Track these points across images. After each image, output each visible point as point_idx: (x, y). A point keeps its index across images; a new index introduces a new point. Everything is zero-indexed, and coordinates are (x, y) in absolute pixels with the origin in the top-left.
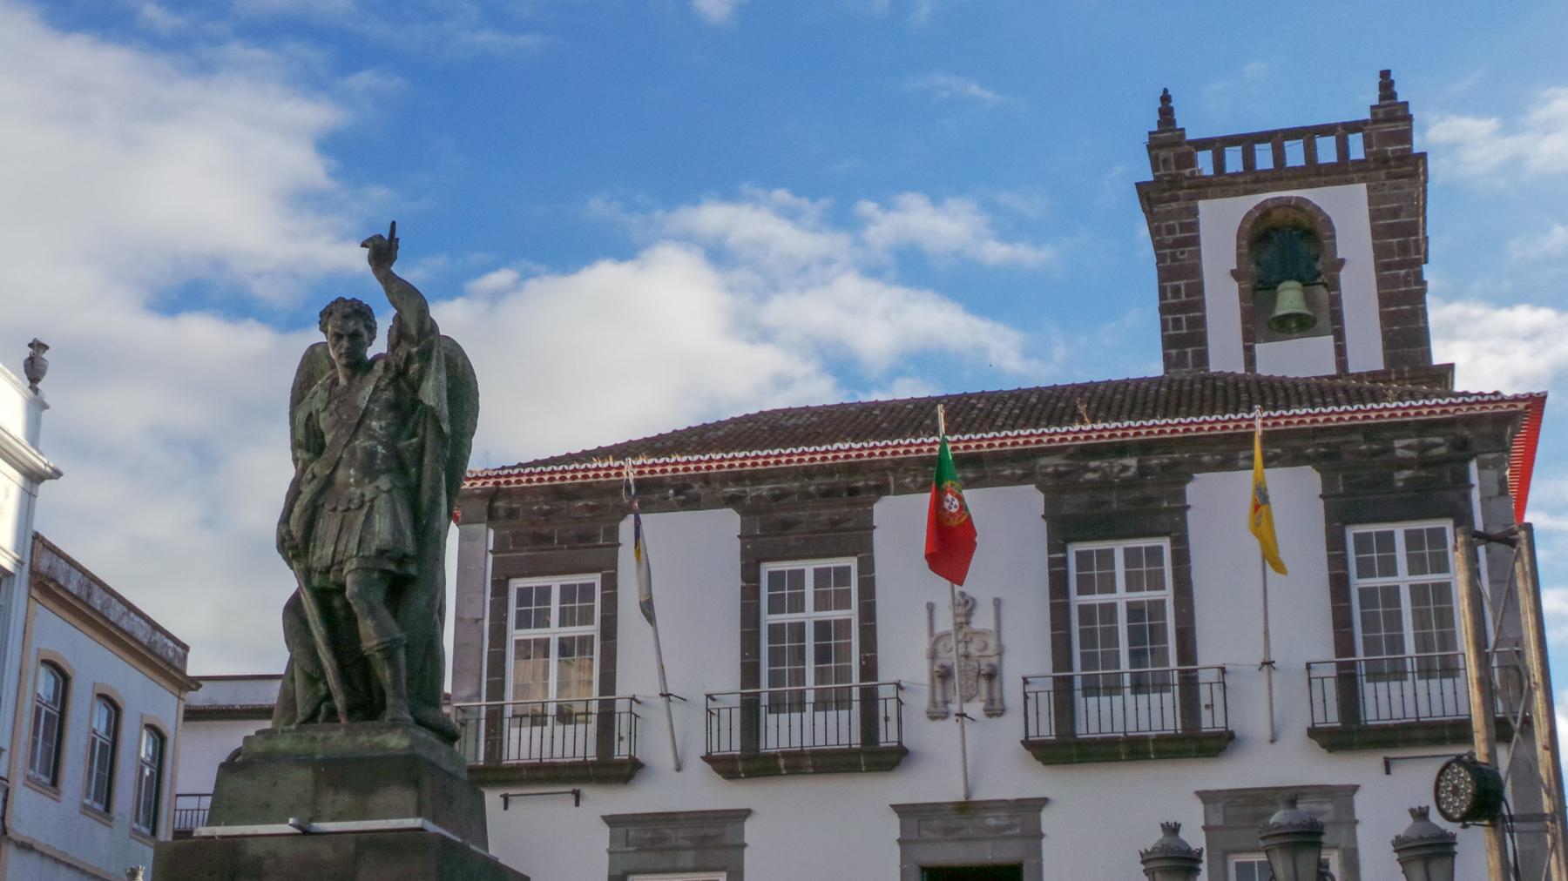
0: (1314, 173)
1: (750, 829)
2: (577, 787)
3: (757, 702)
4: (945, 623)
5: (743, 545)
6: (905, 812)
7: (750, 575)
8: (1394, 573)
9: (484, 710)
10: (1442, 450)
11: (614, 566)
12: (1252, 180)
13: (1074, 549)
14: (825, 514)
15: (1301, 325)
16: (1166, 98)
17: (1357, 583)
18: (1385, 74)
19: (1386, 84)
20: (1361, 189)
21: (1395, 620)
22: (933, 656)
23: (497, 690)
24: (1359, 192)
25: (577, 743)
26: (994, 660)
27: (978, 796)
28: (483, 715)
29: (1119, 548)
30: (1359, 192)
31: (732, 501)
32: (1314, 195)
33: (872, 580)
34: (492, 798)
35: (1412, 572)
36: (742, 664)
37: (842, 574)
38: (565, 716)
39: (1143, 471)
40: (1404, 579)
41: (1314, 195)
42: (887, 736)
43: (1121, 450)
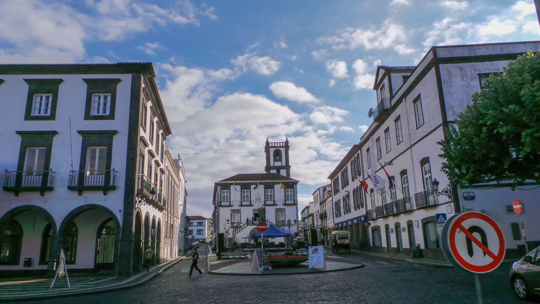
4: (256, 195)
7: (241, 191)
15: (278, 161)
20: (284, 148)
22: (255, 198)
23: (221, 200)
24: (284, 149)
25: (228, 204)
30: (284, 149)
31: (240, 185)
34: (221, 208)
40: (289, 193)
43: (270, 183)
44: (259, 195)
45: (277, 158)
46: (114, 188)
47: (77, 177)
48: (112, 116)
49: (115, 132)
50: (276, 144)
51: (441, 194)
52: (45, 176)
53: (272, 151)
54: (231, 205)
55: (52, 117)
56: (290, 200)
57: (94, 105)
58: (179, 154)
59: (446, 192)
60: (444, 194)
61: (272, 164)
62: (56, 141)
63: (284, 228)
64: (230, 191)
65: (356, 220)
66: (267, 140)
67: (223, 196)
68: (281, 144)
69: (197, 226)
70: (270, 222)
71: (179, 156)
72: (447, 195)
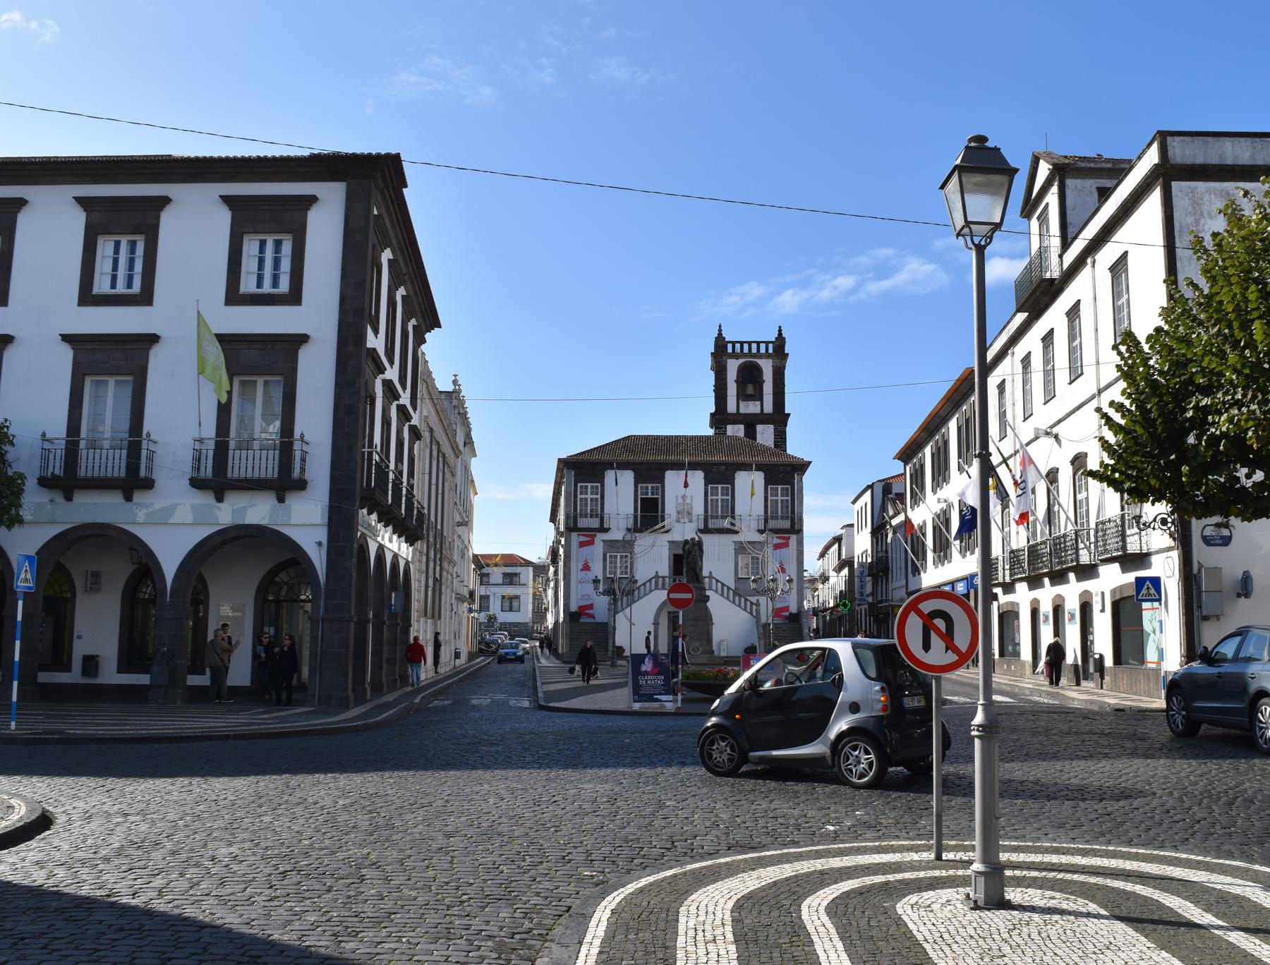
0: (759, 355)
4: (680, 501)
7: (636, 487)
11: (603, 481)
12: (742, 355)
13: (710, 486)
16: (720, 326)
17: (770, 498)
18: (780, 327)
19: (780, 330)
22: (677, 508)
23: (575, 509)
29: (720, 486)
32: (759, 361)
37: (657, 488)
39: (726, 469)
41: (759, 361)
44: (688, 501)
45: (750, 389)
46: (301, 485)
47: (211, 453)
48: (294, 297)
49: (303, 339)
50: (746, 346)
51: (1149, 526)
52: (134, 449)
53: (733, 366)
54: (606, 526)
55: (145, 298)
56: (782, 518)
57: (249, 264)
58: (455, 376)
59: (1164, 522)
60: (1157, 527)
61: (731, 407)
62: (158, 360)
63: (758, 600)
64: (603, 486)
65: (962, 584)
66: (720, 334)
67: (581, 499)
68: (763, 347)
69: (503, 584)
70: (717, 581)
71: (455, 382)
72: (1165, 530)
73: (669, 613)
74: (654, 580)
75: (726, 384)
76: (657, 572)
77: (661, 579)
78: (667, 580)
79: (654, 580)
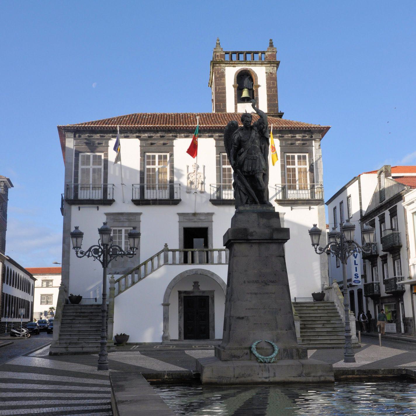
1: (142, 218)
2: (98, 206)
3: (144, 187)
5: (141, 148)
6: (179, 214)
8: (294, 165)
9: (73, 185)
10: (307, 138)
14: (162, 142)
21: (294, 176)
23: (76, 180)
25: (98, 195)
26: (203, 180)
27: (198, 212)
28: (73, 187)
33: (173, 159)
35: (298, 165)
36: (140, 177)
38: (94, 188)
42: (176, 197)
44: (201, 170)
54: (109, 197)
73: (180, 292)
74: (162, 255)
75: (224, 89)
76: (166, 245)
77: (170, 254)
78: (177, 253)
79: (162, 255)
